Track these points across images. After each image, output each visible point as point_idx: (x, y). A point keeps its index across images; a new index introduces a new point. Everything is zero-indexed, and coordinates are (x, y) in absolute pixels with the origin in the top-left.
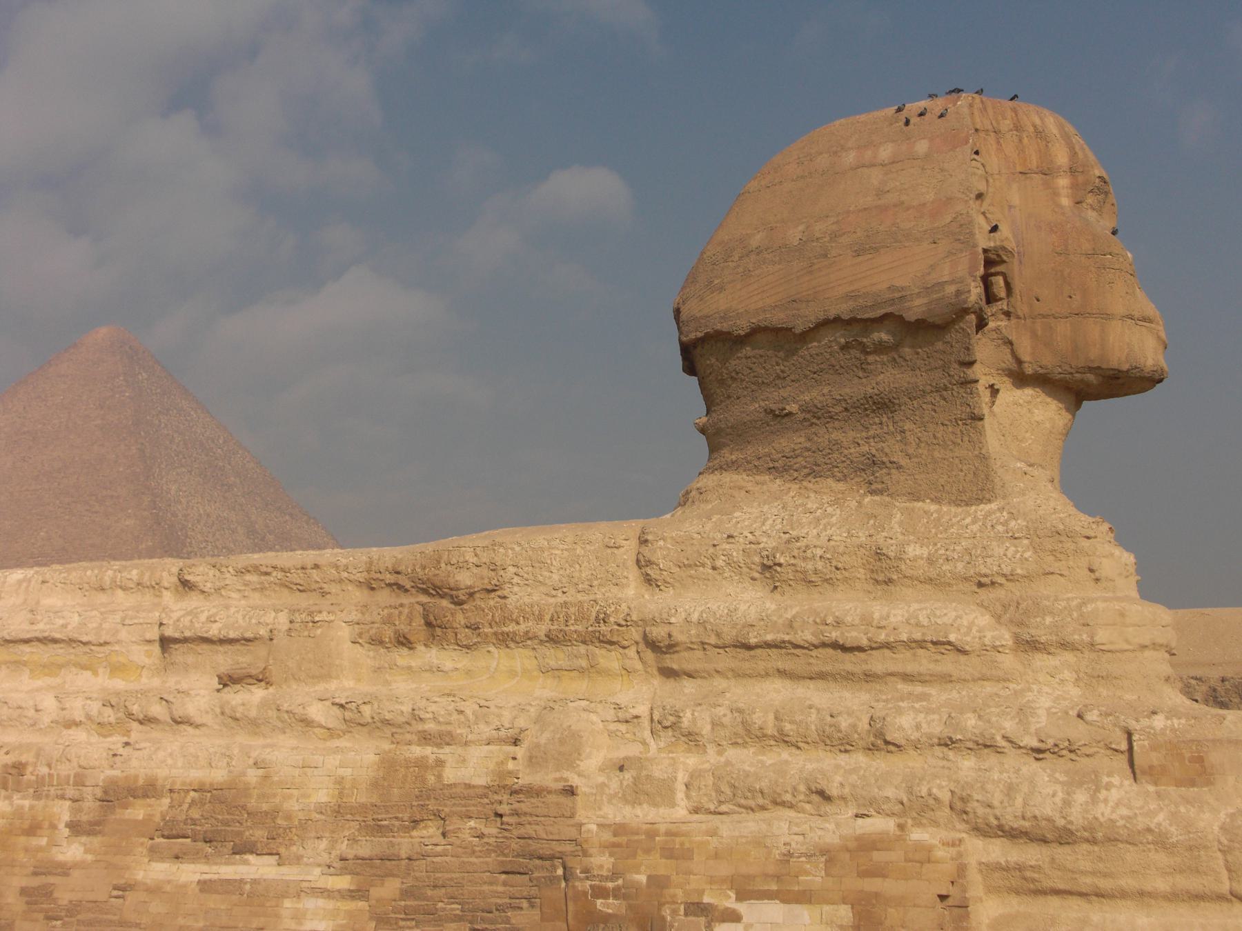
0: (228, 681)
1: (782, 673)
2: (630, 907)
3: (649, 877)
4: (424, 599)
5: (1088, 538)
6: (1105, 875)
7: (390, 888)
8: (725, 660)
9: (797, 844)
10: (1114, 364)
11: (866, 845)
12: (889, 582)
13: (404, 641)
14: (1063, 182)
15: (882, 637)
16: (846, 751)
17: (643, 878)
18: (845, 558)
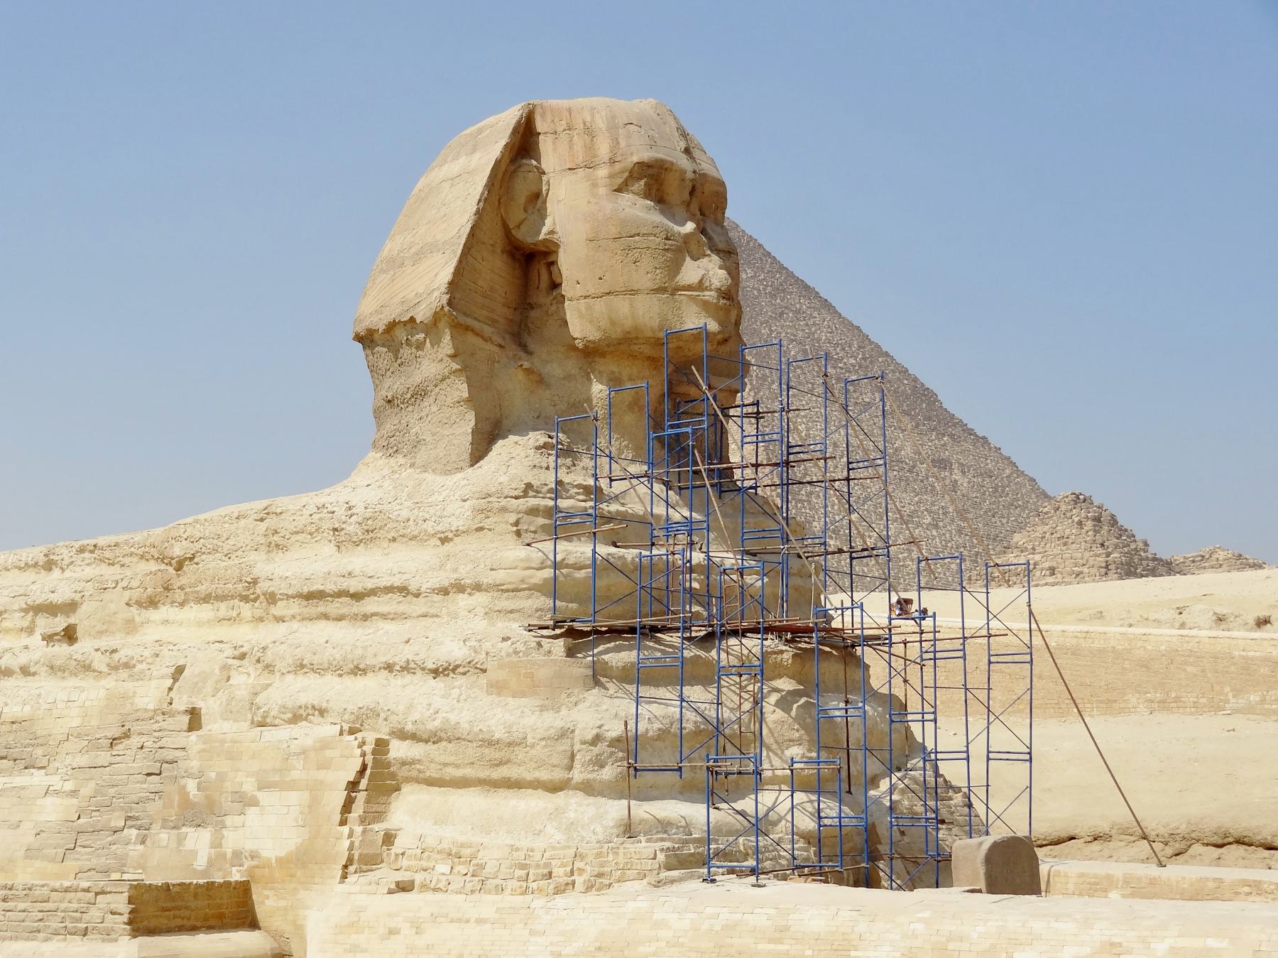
0: (49, 638)
1: (326, 616)
2: (207, 797)
3: (218, 774)
4: (163, 567)
5: (516, 498)
6: (457, 766)
7: (88, 789)
8: (295, 607)
9: (295, 747)
10: (649, 334)
11: (324, 745)
12: (394, 540)
13: (152, 603)
14: (603, 172)
15: (370, 584)
16: (340, 675)
17: (213, 775)
18: (370, 522)
